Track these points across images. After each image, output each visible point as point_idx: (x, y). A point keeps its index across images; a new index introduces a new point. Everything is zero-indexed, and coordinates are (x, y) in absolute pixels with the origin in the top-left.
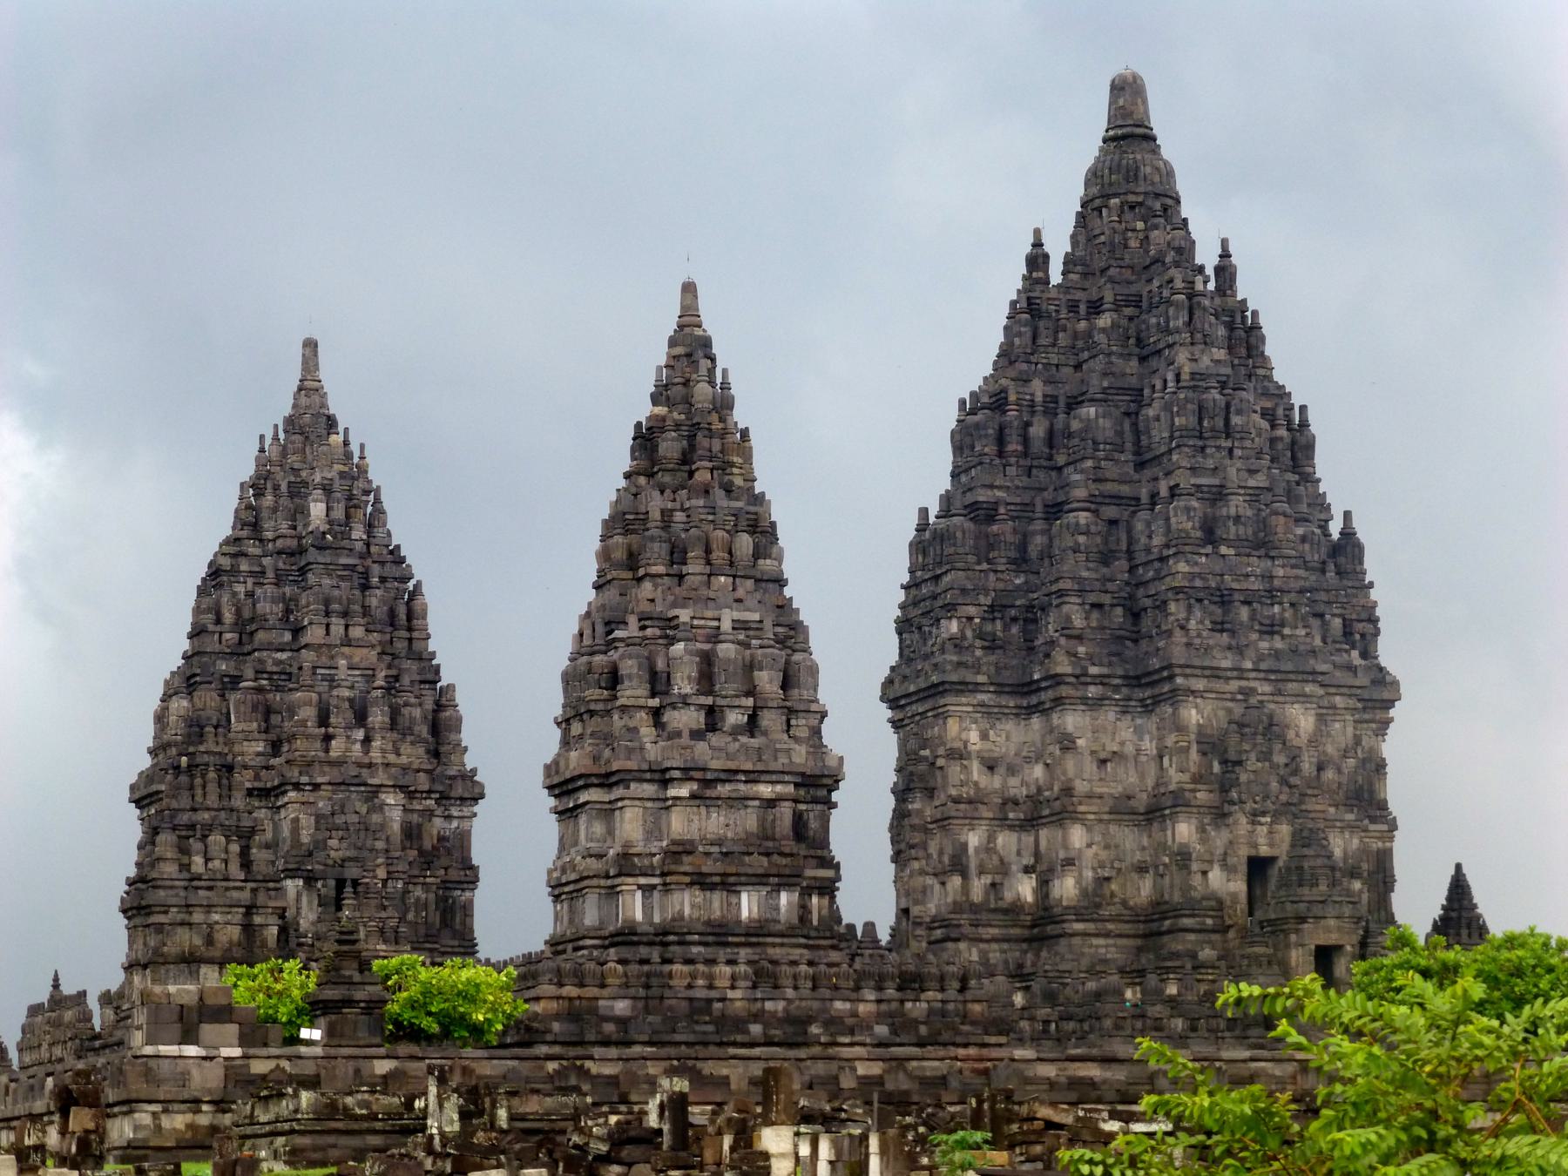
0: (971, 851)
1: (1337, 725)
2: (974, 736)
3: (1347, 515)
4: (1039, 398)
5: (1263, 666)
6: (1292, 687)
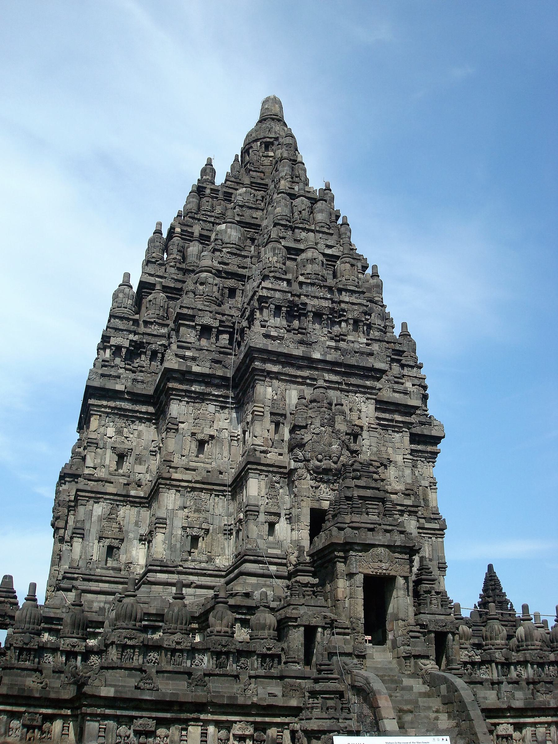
0: (94, 519)
1: (397, 435)
2: (111, 431)
3: (404, 325)
4: (196, 234)
5: (329, 358)
6: (353, 381)
